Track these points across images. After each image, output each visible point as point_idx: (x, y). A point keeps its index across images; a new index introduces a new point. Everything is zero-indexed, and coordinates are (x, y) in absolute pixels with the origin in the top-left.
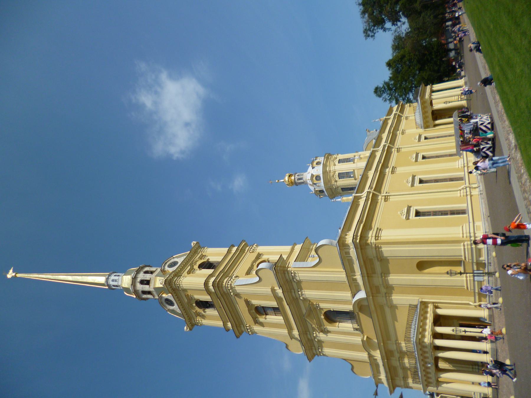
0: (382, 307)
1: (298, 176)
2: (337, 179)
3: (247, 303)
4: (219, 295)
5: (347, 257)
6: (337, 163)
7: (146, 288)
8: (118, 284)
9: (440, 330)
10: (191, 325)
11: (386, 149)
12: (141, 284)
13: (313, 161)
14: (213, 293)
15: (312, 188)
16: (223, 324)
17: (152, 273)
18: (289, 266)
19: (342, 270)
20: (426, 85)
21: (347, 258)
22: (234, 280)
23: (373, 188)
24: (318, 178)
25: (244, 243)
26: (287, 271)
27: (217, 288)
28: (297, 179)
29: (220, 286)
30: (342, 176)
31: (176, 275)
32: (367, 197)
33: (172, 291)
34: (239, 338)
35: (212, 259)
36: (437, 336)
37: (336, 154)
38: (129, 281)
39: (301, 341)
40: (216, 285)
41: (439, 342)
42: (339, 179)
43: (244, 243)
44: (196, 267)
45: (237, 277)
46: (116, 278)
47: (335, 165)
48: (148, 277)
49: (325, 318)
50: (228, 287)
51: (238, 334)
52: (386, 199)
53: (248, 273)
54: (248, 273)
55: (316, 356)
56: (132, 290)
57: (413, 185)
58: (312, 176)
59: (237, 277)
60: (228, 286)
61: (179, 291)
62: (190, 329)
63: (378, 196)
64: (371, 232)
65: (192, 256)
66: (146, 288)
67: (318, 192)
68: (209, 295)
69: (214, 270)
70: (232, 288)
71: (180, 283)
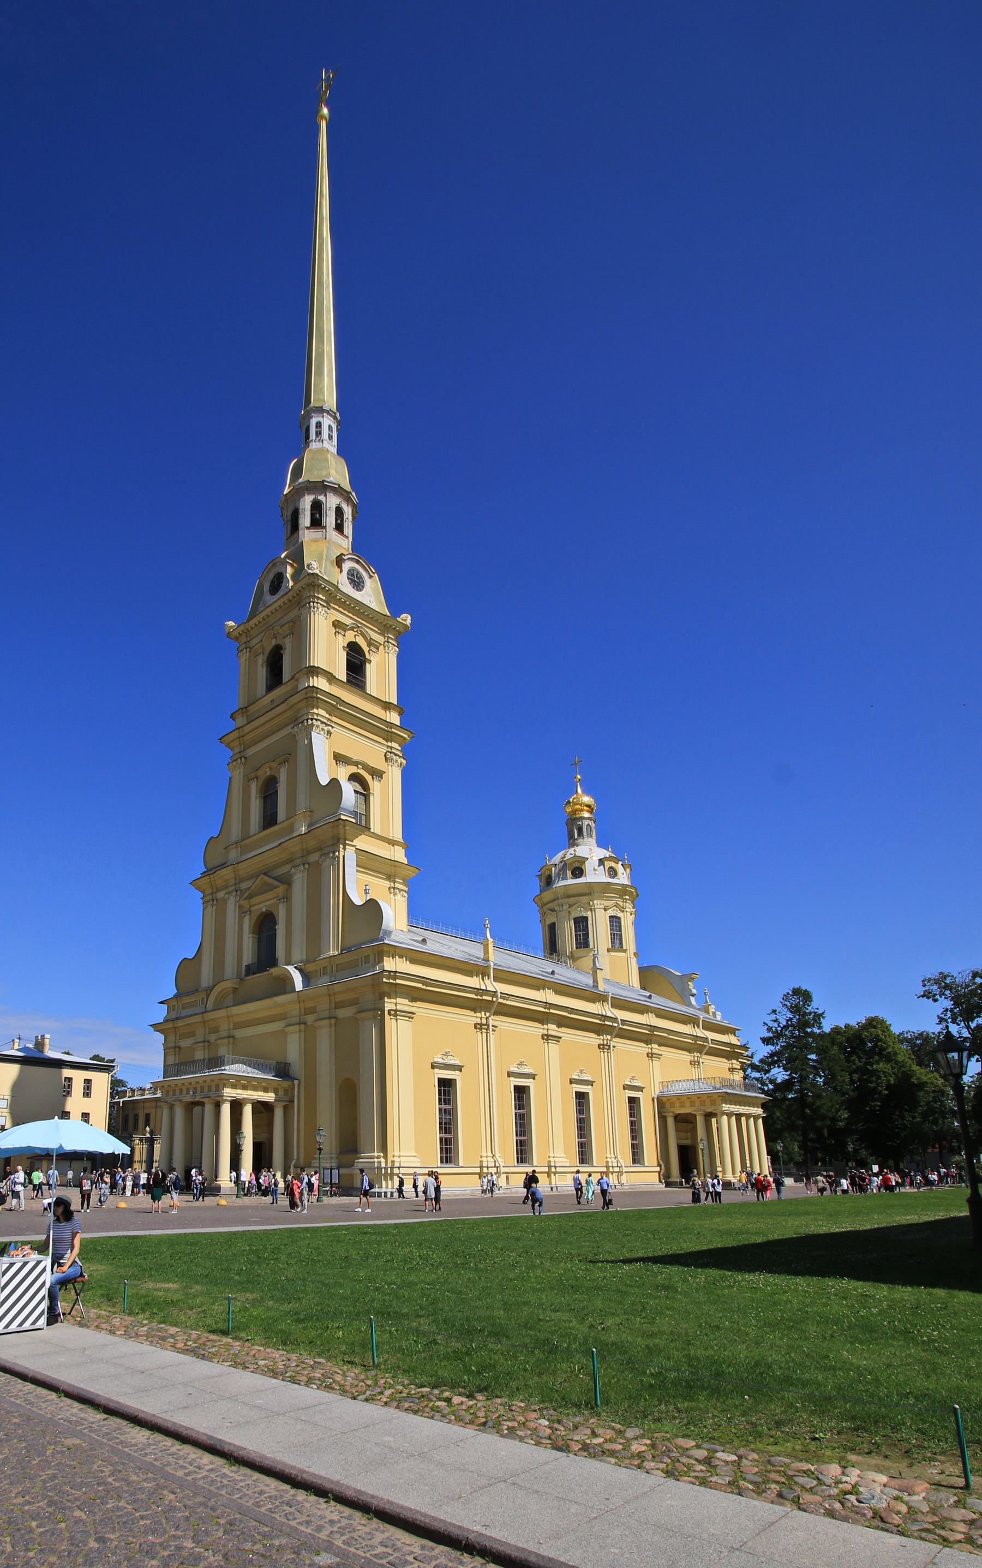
7: (305, 520)
9: (248, 1111)
12: (311, 505)
14: (297, 686)
17: (339, 528)
20: (764, 1106)
22: (323, 729)
23: (505, 1002)
25: (406, 736)
27: (304, 696)
32: (486, 992)
35: (370, 670)
36: (237, 1106)
40: (309, 695)
41: (226, 1109)
43: (406, 736)
45: (329, 733)
48: (330, 519)
53: (339, 758)
54: (339, 758)
57: (510, 1074)
59: (329, 733)
64: (406, 1001)
65: (376, 620)
66: (305, 520)
68: (293, 678)
69: (345, 681)
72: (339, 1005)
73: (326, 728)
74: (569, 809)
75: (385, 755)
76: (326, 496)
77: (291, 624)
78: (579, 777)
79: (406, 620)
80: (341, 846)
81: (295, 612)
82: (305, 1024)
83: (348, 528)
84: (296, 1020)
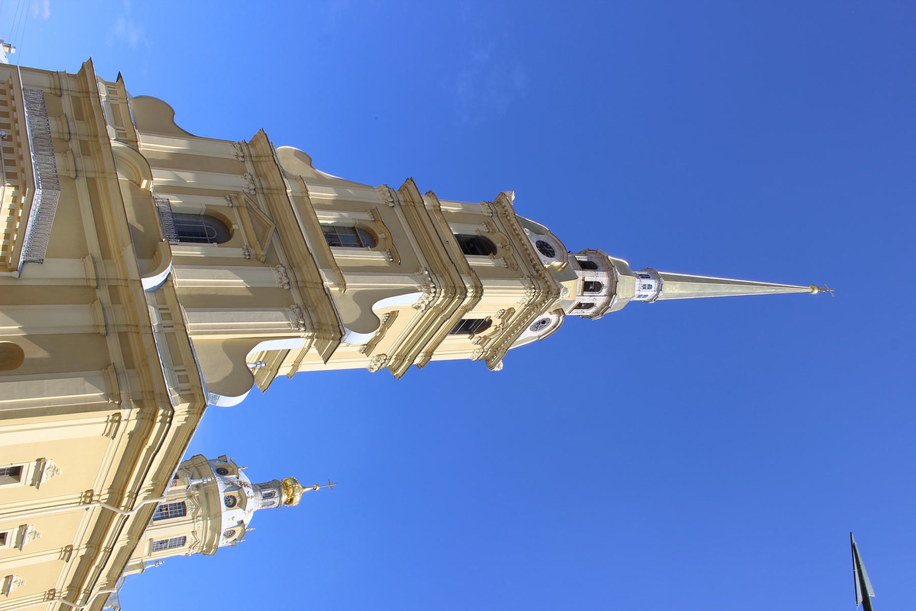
0: (105, 252)
1: (274, 503)
2: (188, 502)
3: (393, 255)
4: (452, 269)
5: (184, 370)
6: (190, 537)
7: (590, 276)
8: (641, 281)
10: (503, 204)
11: (82, 596)
13: (241, 537)
15: (244, 478)
16: (441, 207)
17: (579, 306)
18: (309, 340)
19: (193, 338)
21: (184, 369)
22: (423, 302)
24: (231, 503)
26: (313, 329)
27: (457, 285)
28: (276, 496)
29: (449, 288)
30: (179, 510)
31: (537, 306)
33: (544, 274)
34: (408, 179)
37: (190, 555)
38: (621, 287)
39: (282, 174)
42: (183, 503)
43: (398, 373)
44: (496, 322)
45: (418, 308)
46: (644, 292)
47: (193, 532)
48: (587, 299)
49: (231, 225)
50: (434, 287)
51: (411, 187)
52: (88, 497)
53: (392, 316)
55: (248, 142)
56: (617, 270)
57: (23, 528)
58: (243, 505)
59: (418, 308)
60: (434, 290)
61: (530, 276)
62: (503, 194)
63: (109, 501)
67: (230, 470)
70: (427, 286)
71: (530, 291)
72: (123, 337)
73: (423, 306)
74: (289, 483)
75: (383, 354)
76: (605, 296)
77: (516, 267)
78: (318, 488)
79: (499, 367)
80: (311, 334)
81: (526, 272)
82: (97, 287)
83: (576, 312)
84: (102, 275)
